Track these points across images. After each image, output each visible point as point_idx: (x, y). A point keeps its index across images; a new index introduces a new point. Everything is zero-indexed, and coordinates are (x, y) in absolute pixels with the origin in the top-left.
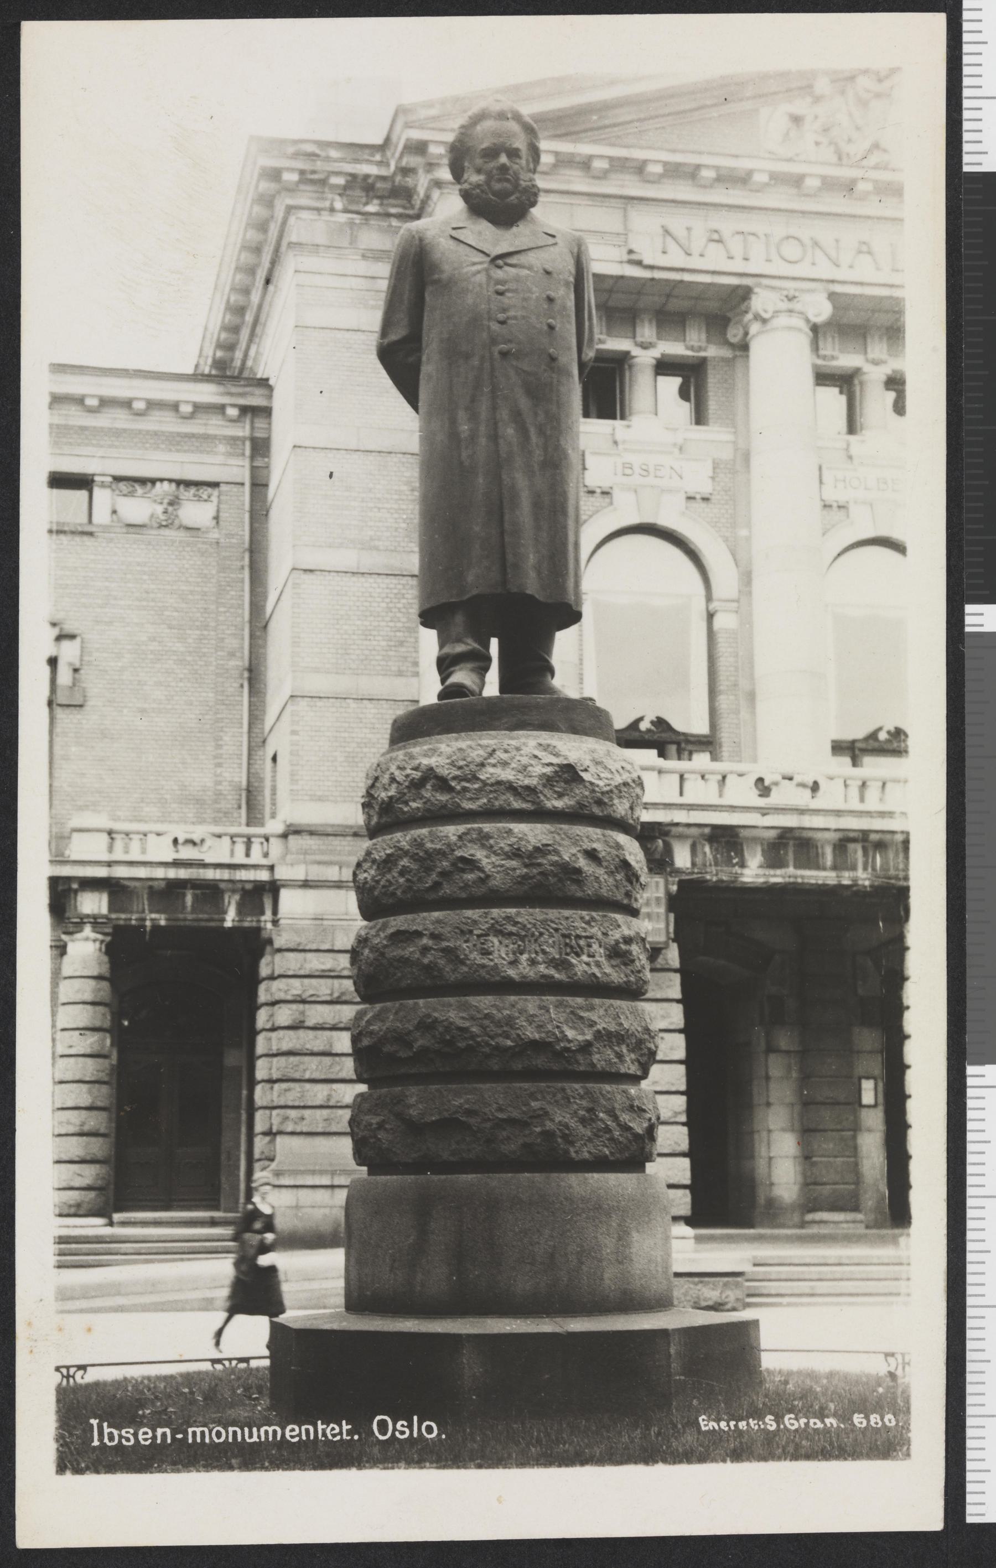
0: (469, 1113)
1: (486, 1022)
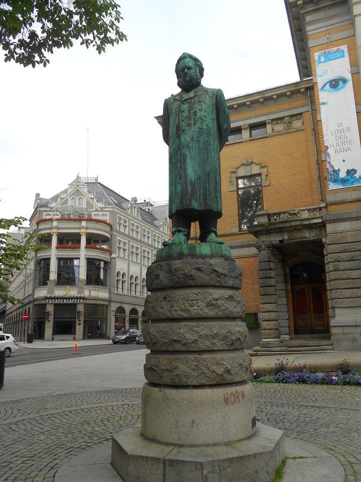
0: (156, 366)
1: (161, 333)
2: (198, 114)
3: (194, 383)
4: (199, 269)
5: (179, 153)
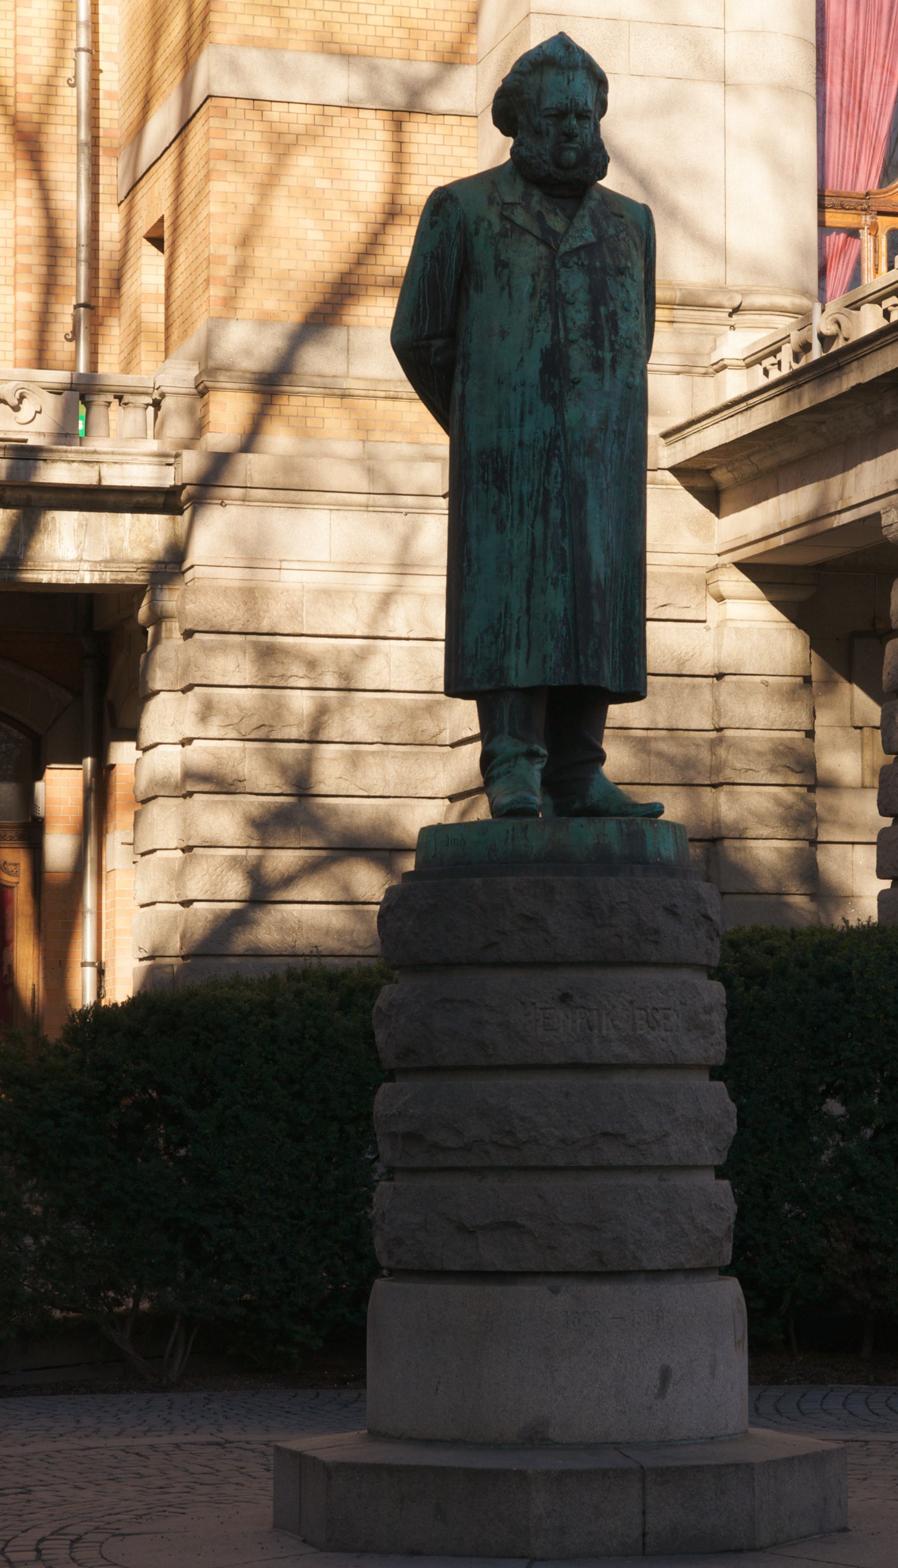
2: (623, 326)
3: (658, 1263)
4: (671, 911)
5: (556, 467)
